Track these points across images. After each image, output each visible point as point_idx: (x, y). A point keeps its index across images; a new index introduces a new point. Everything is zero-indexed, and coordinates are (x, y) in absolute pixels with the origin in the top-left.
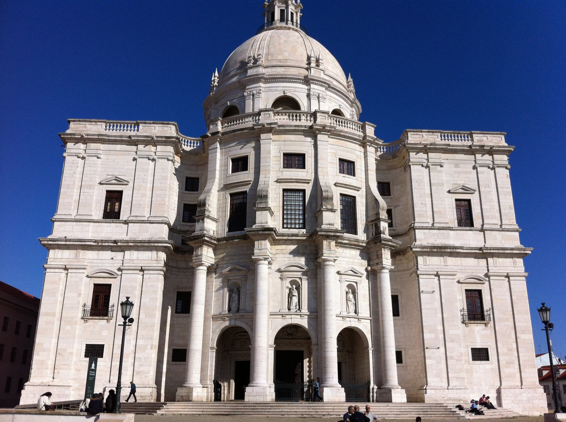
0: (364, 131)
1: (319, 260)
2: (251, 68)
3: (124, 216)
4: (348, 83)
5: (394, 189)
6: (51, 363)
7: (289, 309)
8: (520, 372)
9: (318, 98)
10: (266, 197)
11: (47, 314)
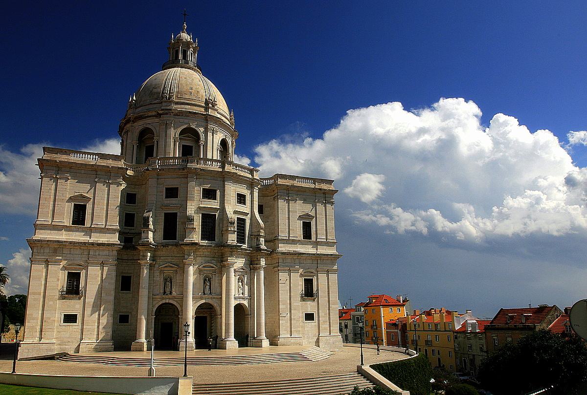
0: (253, 175)
1: (225, 263)
2: (165, 102)
3: (88, 224)
4: (231, 116)
5: (265, 209)
6: (38, 328)
7: (204, 293)
8: (330, 327)
9: (213, 131)
10: (192, 220)
11: (34, 294)
